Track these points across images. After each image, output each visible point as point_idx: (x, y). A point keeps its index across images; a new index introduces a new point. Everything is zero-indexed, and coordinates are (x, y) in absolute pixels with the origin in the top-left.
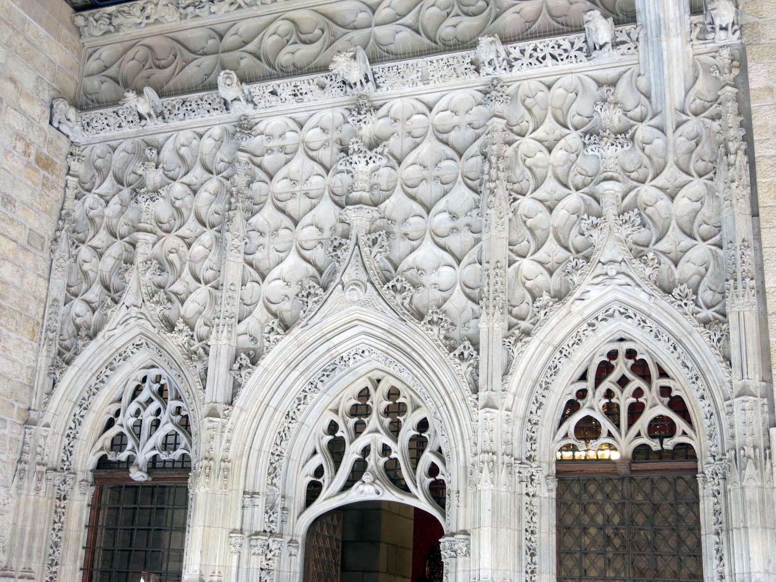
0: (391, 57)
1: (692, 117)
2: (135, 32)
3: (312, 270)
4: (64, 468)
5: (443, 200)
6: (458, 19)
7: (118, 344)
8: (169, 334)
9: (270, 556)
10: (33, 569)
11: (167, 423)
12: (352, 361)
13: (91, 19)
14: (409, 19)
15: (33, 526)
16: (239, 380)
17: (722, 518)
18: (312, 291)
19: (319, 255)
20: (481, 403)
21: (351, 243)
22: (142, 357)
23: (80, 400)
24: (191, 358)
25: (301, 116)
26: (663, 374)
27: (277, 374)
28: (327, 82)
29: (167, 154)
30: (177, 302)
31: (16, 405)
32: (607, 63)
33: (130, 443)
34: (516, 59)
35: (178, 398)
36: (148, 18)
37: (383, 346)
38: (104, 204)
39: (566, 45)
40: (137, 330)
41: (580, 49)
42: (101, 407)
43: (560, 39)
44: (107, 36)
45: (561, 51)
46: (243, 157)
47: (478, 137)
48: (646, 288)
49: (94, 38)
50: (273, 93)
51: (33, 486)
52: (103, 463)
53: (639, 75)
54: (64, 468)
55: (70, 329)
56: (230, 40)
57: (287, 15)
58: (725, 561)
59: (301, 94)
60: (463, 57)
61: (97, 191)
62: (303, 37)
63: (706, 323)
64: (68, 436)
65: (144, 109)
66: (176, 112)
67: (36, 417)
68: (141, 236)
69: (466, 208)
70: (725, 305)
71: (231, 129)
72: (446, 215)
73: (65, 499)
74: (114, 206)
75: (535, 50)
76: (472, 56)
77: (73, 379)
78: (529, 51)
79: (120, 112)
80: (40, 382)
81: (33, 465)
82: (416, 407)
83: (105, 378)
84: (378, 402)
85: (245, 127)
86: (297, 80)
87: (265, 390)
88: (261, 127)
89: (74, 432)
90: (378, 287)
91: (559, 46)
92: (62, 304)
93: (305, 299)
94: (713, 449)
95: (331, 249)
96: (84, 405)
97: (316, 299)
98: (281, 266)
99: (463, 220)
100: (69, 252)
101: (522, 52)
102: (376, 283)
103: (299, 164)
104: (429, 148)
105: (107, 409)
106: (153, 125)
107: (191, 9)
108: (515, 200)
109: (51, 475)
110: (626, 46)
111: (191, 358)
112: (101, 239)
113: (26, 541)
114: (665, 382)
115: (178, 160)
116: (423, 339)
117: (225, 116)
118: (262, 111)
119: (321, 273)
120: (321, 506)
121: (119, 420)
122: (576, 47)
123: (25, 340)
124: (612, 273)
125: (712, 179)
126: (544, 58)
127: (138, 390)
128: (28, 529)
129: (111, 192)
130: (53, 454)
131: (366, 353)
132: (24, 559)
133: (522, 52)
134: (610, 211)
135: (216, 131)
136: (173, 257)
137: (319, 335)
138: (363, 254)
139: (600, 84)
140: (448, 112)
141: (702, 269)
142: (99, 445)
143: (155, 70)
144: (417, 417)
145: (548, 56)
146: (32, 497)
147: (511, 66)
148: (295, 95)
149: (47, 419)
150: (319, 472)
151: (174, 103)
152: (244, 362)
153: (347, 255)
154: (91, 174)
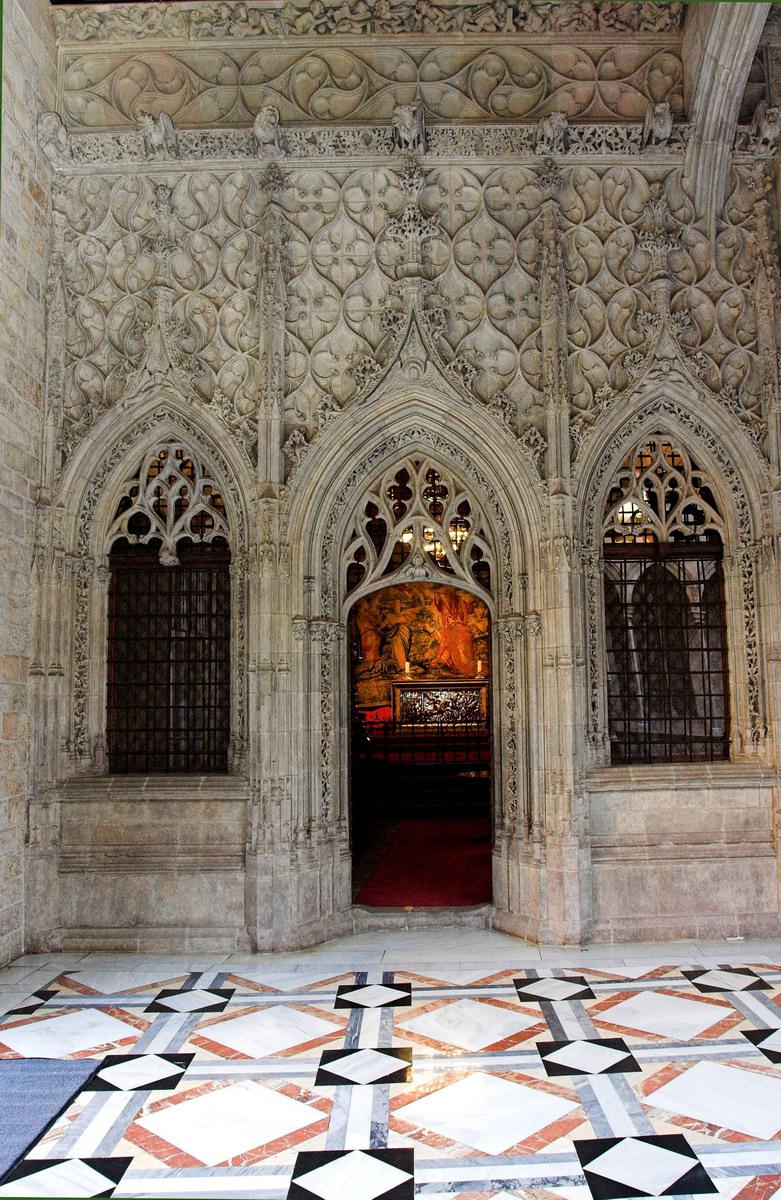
0: (317, 121)
1: (731, 225)
2: (129, 43)
3: (362, 344)
4: (81, 553)
5: (499, 281)
6: (153, 94)
7: (136, 415)
8: (206, 406)
9: (327, 641)
10: (62, 663)
11: (197, 503)
12: (401, 442)
13: (77, 16)
14: (103, 88)
15: (59, 616)
16: (293, 459)
17: (753, 595)
18: (368, 366)
19: (373, 330)
20: (552, 489)
21: (407, 317)
22: (161, 430)
23: (94, 476)
24: (234, 433)
25: (340, 174)
26: (695, 467)
27: (332, 453)
28: (375, 136)
29: (181, 199)
30: (209, 369)
31: (29, 481)
32: (658, 161)
33: (155, 523)
34: (574, 142)
35: (206, 475)
36: (151, 27)
37: (437, 429)
38: (105, 250)
39: (623, 134)
40: (160, 399)
41: (635, 141)
42: (116, 485)
43: (618, 126)
44: (92, 42)
45: (617, 140)
46: (276, 210)
47: (530, 220)
48: (697, 385)
49: (75, 42)
50: (312, 141)
51: (54, 574)
52: (120, 546)
53: (683, 176)
54: (81, 553)
55: (73, 395)
56: (251, 72)
57: (317, 52)
58: (756, 631)
59: (344, 146)
60: (522, 130)
61: (92, 233)
62: (338, 81)
63: (745, 420)
64: (83, 517)
65: (156, 139)
66: (194, 148)
67: (48, 496)
68: (161, 291)
69: (523, 291)
70: (760, 407)
71: (257, 178)
72: (501, 297)
73: (85, 587)
74: (118, 252)
75: (593, 134)
76: (531, 131)
77: (87, 454)
78: (587, 134)
79: (122, 141)
80: (49, 456)
81: (51, 550)
82: (458, 492)
83: (121, 453)
84: (418, 483)
85: (274, 179)
86: (340, 130)
87: (320, 470)
88: (293, 179)
89: (89, 512)
90: (440, 366)
91: (617, 134)
92: (62, 365)
93: (361, 375)
94: (745, 535)
95: (385, 323)
96: (98, 481)
97: (373, 375)
98: (329, 337)
99: (518, 305)
100: (66, 305)
101: (581, 134)
102: (437, 363)
103: (344, 229)
104: (485, 225)
105: (121, 487)
106: (161, 161)
107: (206, 25)
108: (571, 288)
109: (69, 561)
110: (678, 145)
111: (234, 433)
112: (105, 294)
113: (52, 635)
114: (696, 474)
115: (191, 206)
116: (487, 425)
117: (250, 162)
118: (295, 160)
119: (374, 349)
120: (364, 589)
121: (138, 500)
122: (632, 138)
123: (31, 406)
124: (666, 369)
125: (748, 287)
126: (600, 145)
127: (159, 467)
128: (53, 620)
129: (111, 236)
130: (70, 541)
131: (416, 434)
132: (52, 654)
133: (581, 134)
134: (663, 309)
135: (239, 178)
136: (198, 318)
137: (374, 414)
138: (422, 331)
139: (650, 183)
140: (499, 189)
141: (740, 373)
142: (115, 527)
143: (159, 95)
144: (460, 500)
145: (604, 144)
146: (53, 586)
147: (567, 148)
148: (336, 147)
149: (62, 499)
150: (360, 554)
151: (193, 137)
152: (297, 440)
153: (404, 330)
154: (83, 211)
